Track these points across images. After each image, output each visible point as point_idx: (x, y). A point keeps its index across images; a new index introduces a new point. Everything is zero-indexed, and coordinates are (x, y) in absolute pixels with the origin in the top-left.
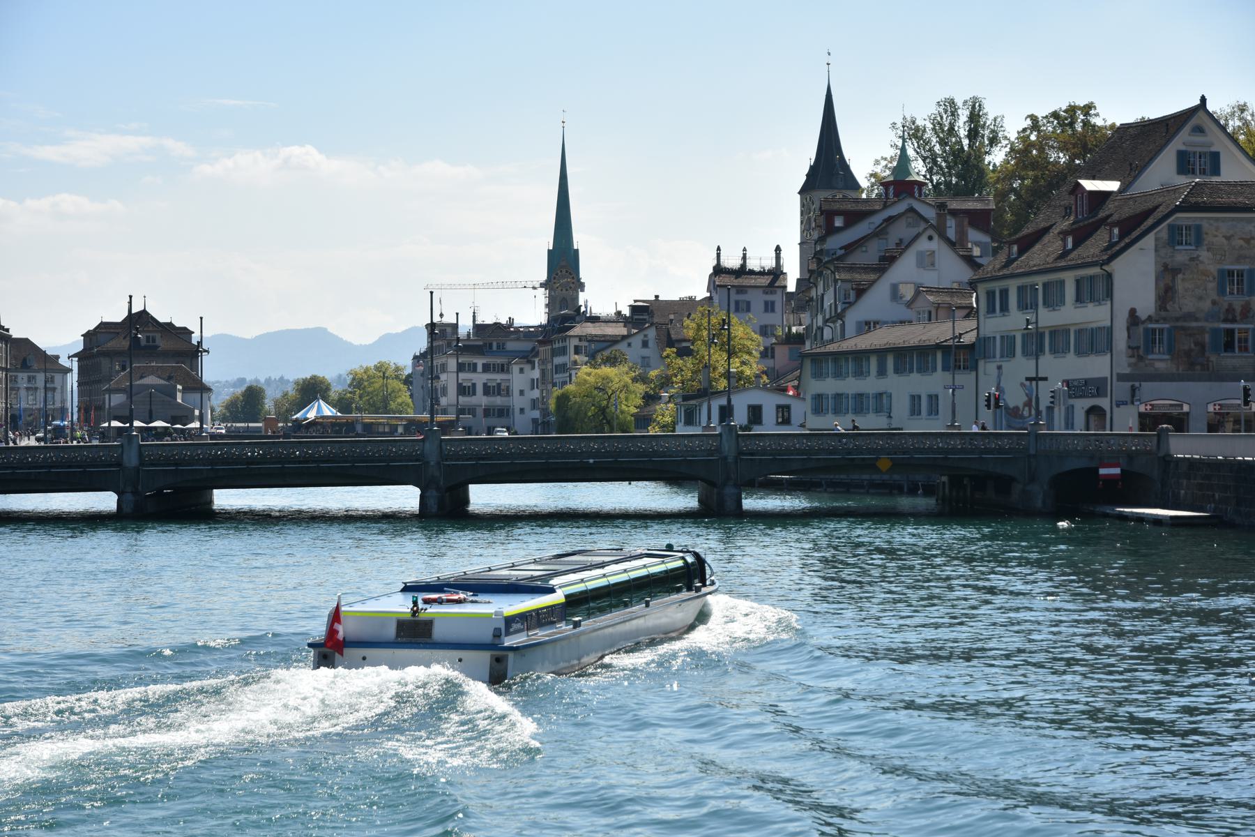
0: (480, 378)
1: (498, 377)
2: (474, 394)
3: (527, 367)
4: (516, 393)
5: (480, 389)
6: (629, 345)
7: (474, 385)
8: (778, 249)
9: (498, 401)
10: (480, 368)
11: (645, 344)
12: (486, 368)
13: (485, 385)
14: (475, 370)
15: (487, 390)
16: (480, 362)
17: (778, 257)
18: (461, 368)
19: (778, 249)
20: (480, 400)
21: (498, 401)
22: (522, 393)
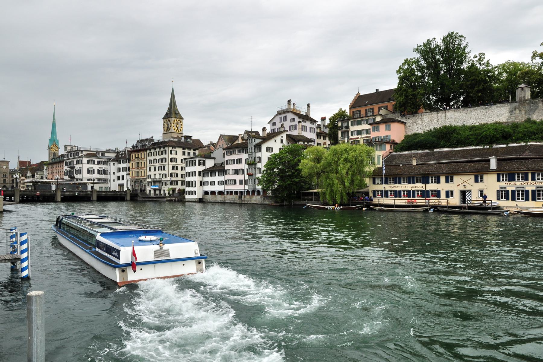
0: (96, 167)
1: (103, 167)
2: (94, 173)
3: (116, 163)
4: (112, 173)
5: (96, 171)
6: (275, 141)
7: (94, 169)
8: (308, 105)
9: (103, 176)
10: (96, 163)
11: (282, 141)
12: (99, 163)
13: (98, 170)
14: (94, 163)
15: (99, 172)
16: (96, 160)
17: (308, 109)
18: (88, 162)
19: (308, 105)
20: (96, 176)
21: (103, 176)
22: (114, 173)
